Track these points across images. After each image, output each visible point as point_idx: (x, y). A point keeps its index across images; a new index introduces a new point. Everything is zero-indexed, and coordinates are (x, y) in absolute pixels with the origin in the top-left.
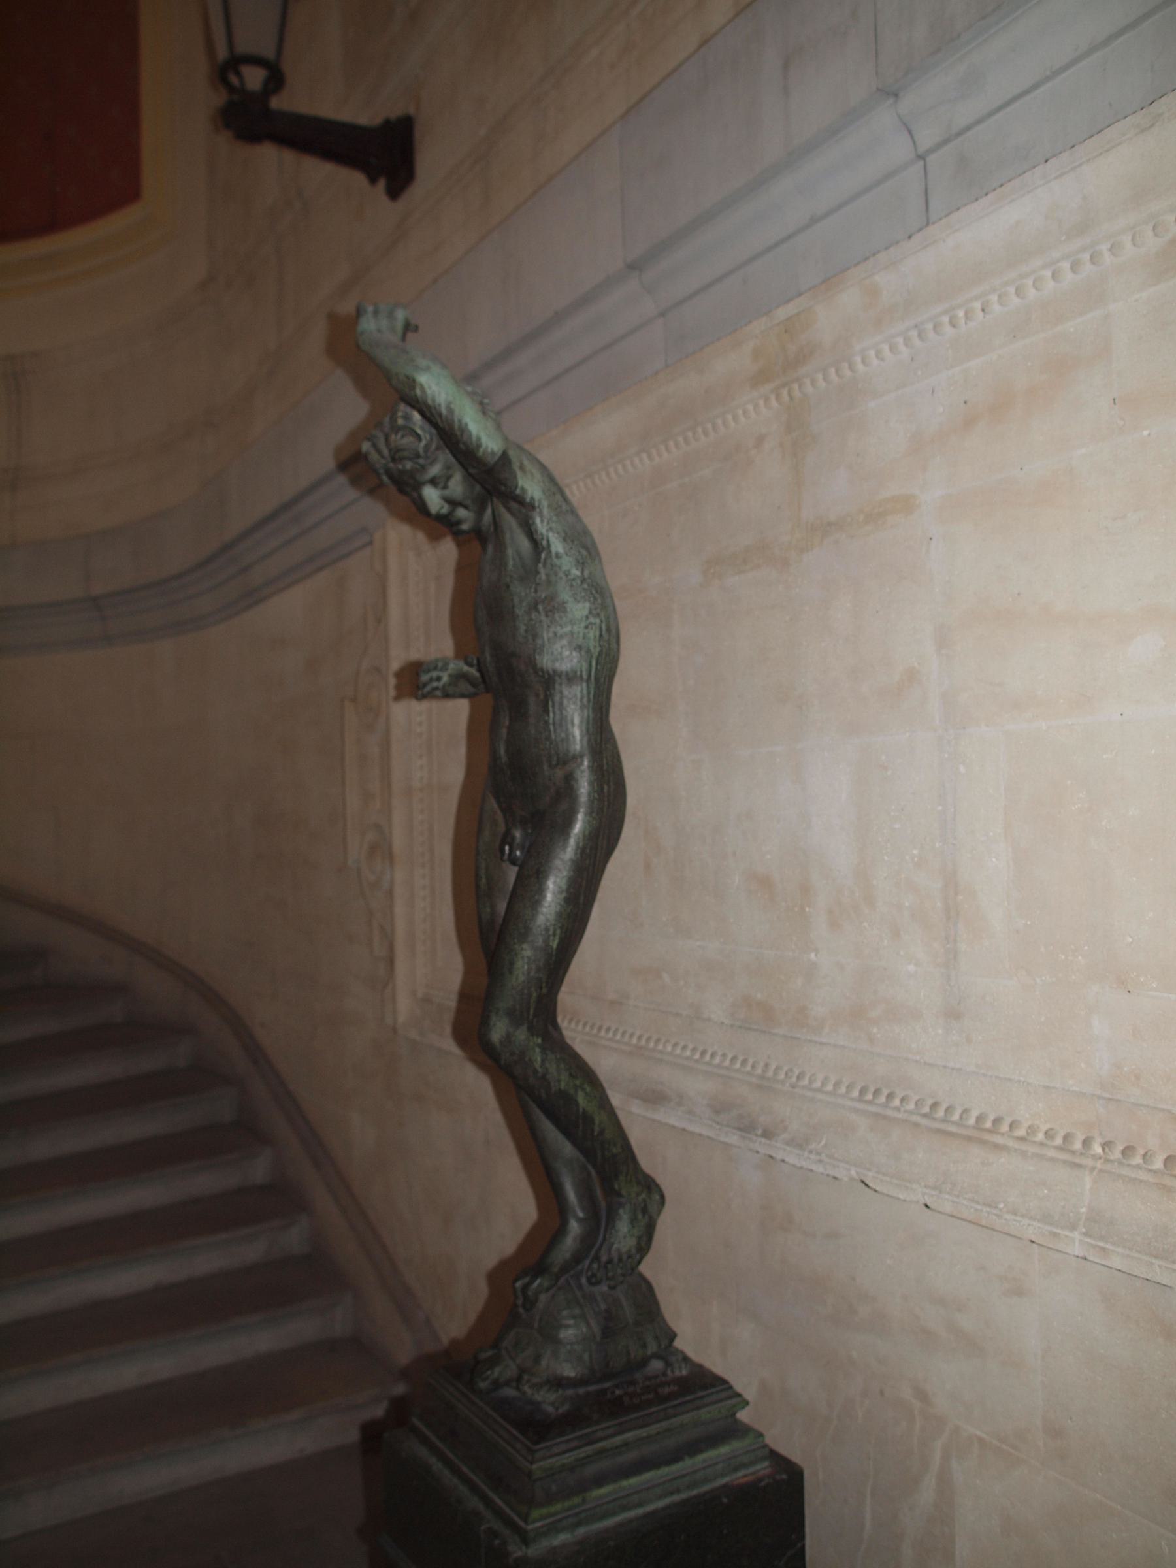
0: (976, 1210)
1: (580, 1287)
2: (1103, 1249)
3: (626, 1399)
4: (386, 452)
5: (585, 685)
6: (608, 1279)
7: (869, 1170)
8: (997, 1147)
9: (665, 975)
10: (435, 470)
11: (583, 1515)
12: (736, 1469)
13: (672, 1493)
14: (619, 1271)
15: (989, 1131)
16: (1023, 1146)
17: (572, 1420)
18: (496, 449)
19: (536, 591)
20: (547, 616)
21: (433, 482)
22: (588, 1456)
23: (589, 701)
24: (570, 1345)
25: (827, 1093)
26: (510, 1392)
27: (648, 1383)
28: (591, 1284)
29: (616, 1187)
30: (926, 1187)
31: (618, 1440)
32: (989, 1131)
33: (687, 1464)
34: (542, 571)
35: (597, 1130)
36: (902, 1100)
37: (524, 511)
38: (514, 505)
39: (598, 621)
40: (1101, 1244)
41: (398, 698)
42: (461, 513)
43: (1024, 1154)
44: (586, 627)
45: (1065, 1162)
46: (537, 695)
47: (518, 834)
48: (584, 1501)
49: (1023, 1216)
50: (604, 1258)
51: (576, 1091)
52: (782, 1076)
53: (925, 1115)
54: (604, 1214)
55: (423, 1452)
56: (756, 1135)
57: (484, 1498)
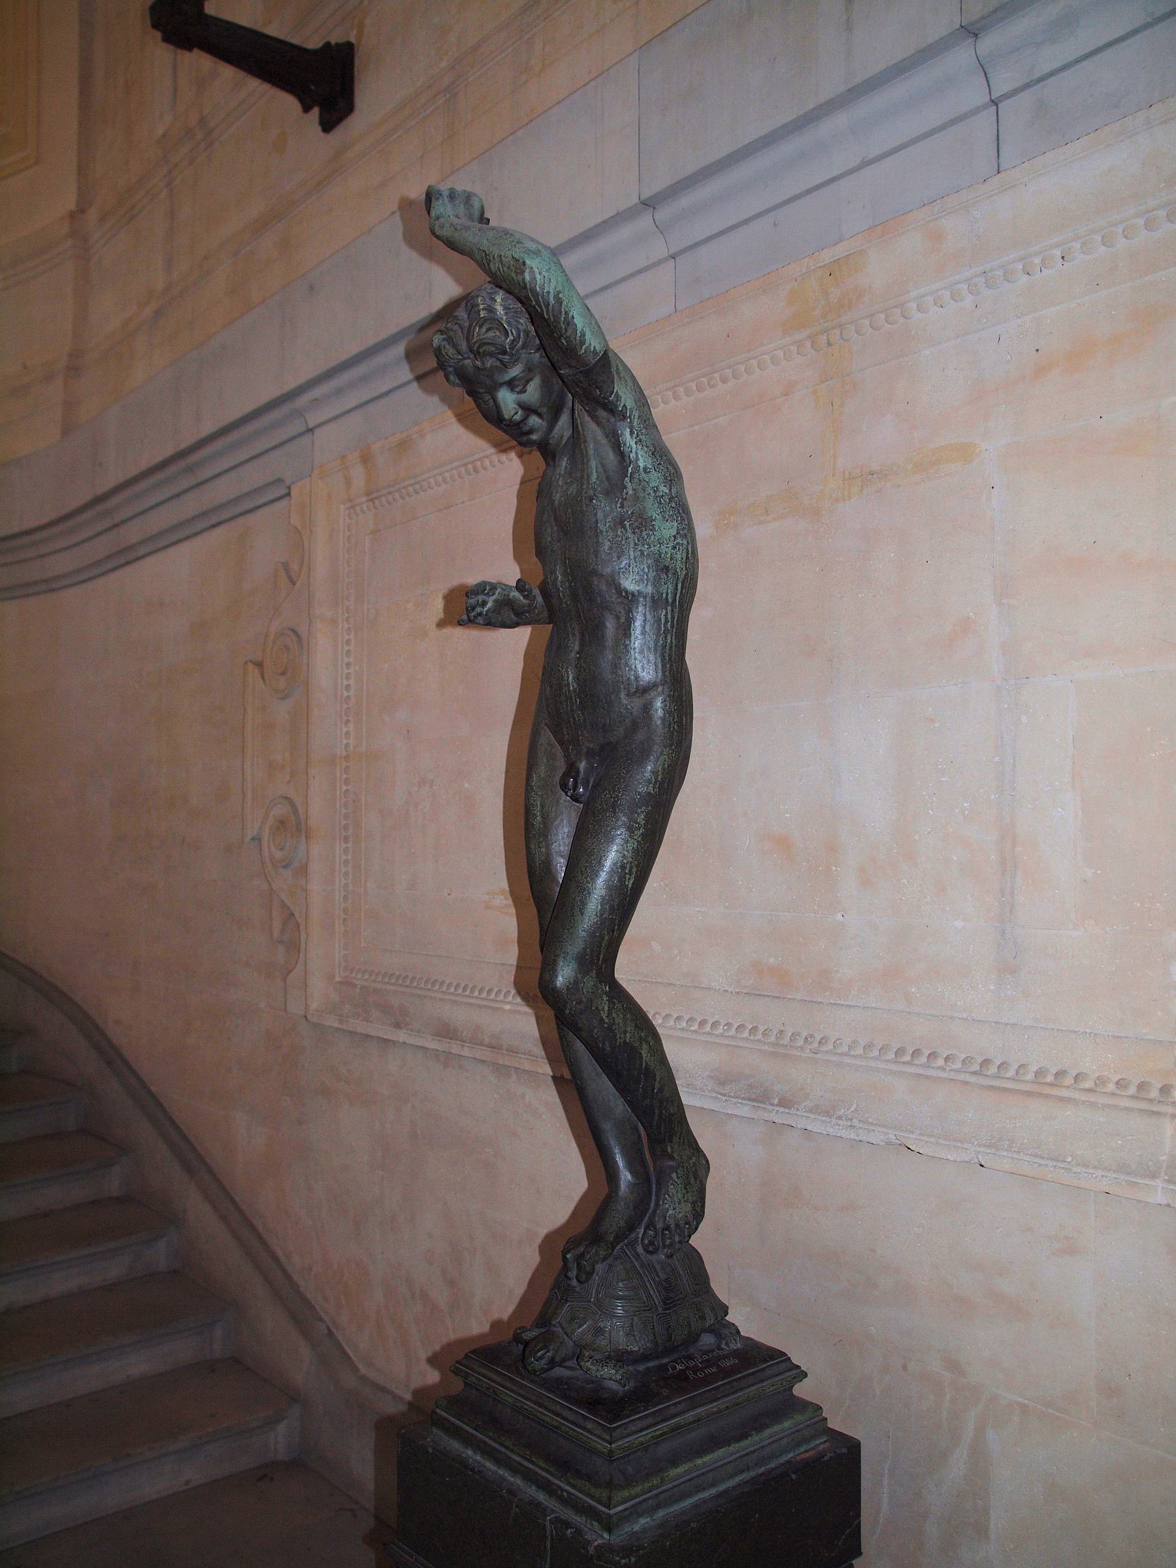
0: (1040, 1165)
1: (637, 1256)
3: (690, 1373)
4: (464, 346)
5: (669, 608)
6: (664, 1246)
7: (913, 1133)
9: (656, 946)
10: (515, 371)
11: (662, 1497)
12: (798, 1445)
13: (742, 1471)
14: (677, 1238)
15: (1052, 1085)
16: (1092, 1098)
17: (640, 1397)
18: (598, 350)
19: (622, 507)
20: (634, 533)
21: (511, 384)
22: (664, 1434)
23: (672, 627)
24: (617, 1323)
25: (855, 1057)
26: (559, 1372)
27: (705, 1357)
28: (651, 1253)
29: (669, 1149)
30: (980, 1146)
31: (690, 1415)
32: (1052, 1085)
33: (754, 1440)
34: (629, 485)
35: (657, 1085)
36: (947, 1059)
37: (613, 420)
38: (602, 413)
39: (685, 542)
41: (441, 624)
42: (534, 420)
43: (1093, 1105)
44: (674, 548)
45: (1141, 1110)
46: (618, 618)
47: (582, 766)
48: (662, 1480)
49: (1095, 1167)
50: (660, 1225)
51: (641, 1045)
52: (800, 1043)
53: (975, 1073)
54: (654, 1180)
55: (455, 1445)
56: (772, 1104)
57: (546, 1486)
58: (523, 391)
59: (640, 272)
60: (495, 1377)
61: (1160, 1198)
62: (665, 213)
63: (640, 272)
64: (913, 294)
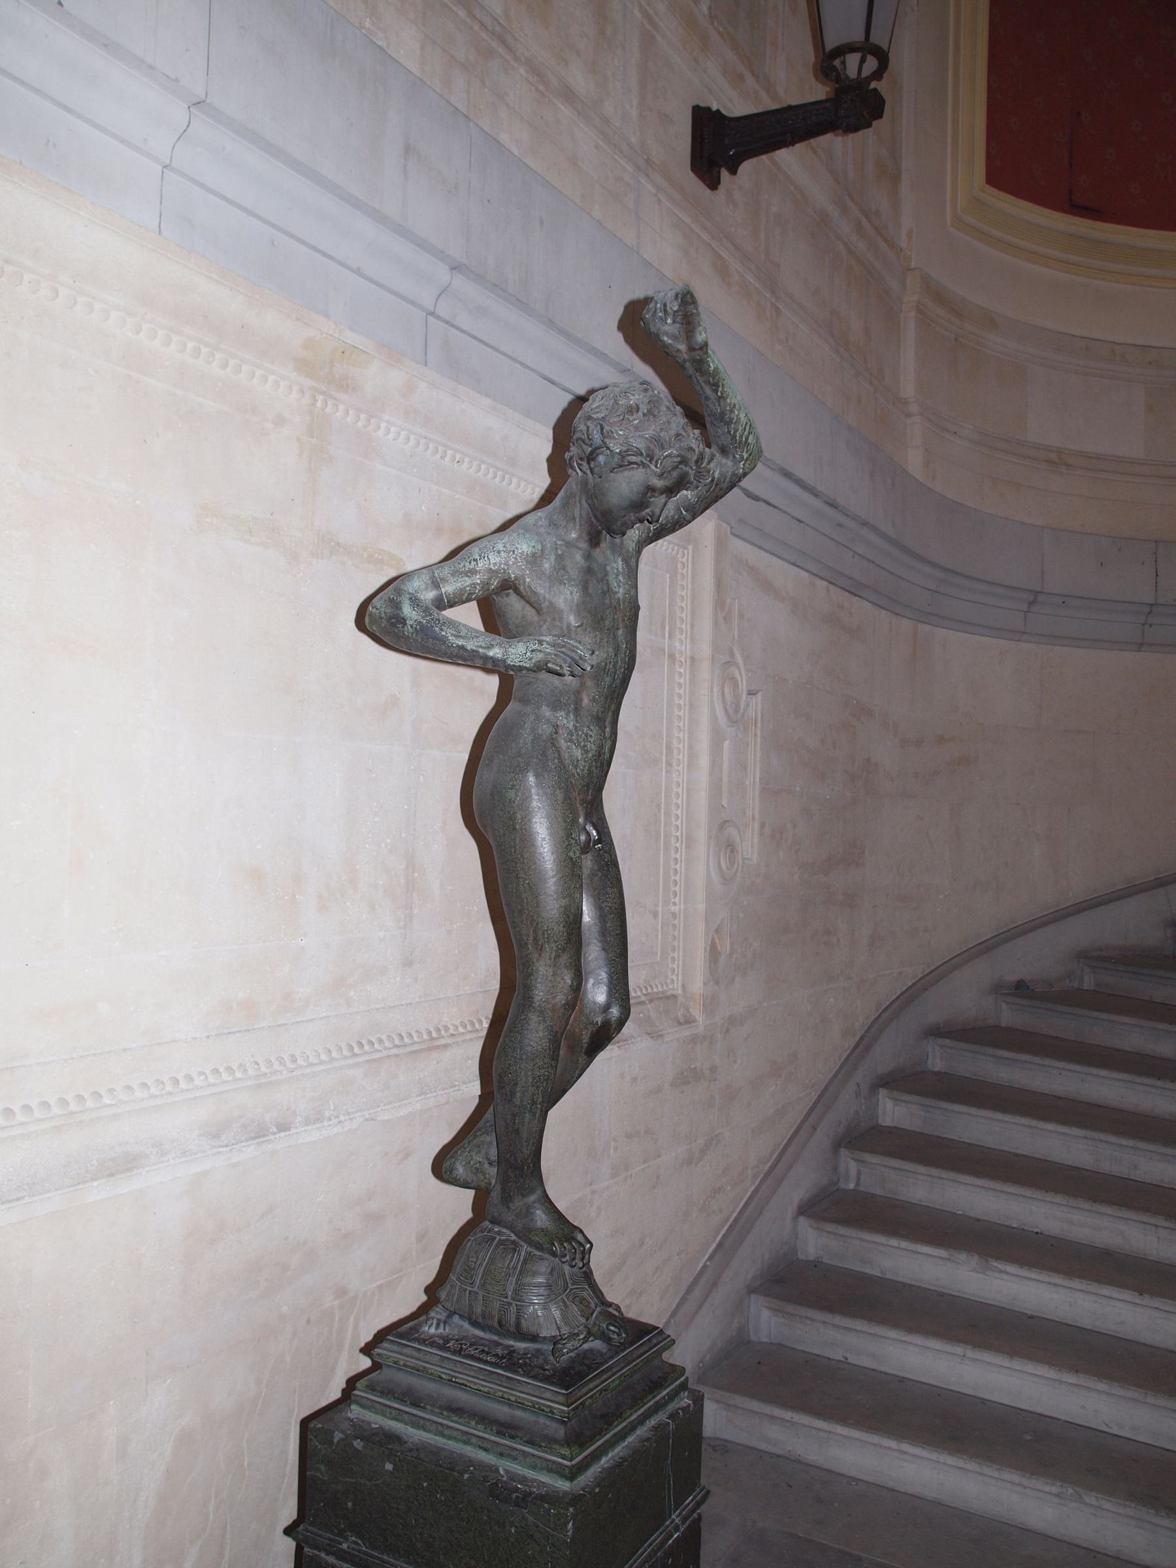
8: (446, 1046)
55: (604, 1461)
60: (595, 1383)
64: (386, 417)
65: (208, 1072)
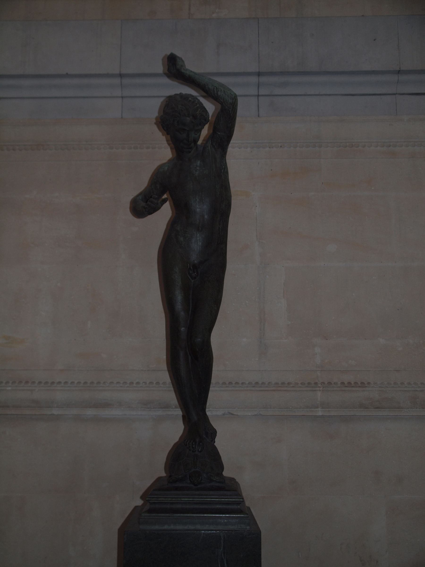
2: (329, 411)
40: (327, 410)
58: (196, 134)
59: (105, 97)
61: (320, 414)
62: (126, 81)
63: (105, 97)
65: (148, 383)
